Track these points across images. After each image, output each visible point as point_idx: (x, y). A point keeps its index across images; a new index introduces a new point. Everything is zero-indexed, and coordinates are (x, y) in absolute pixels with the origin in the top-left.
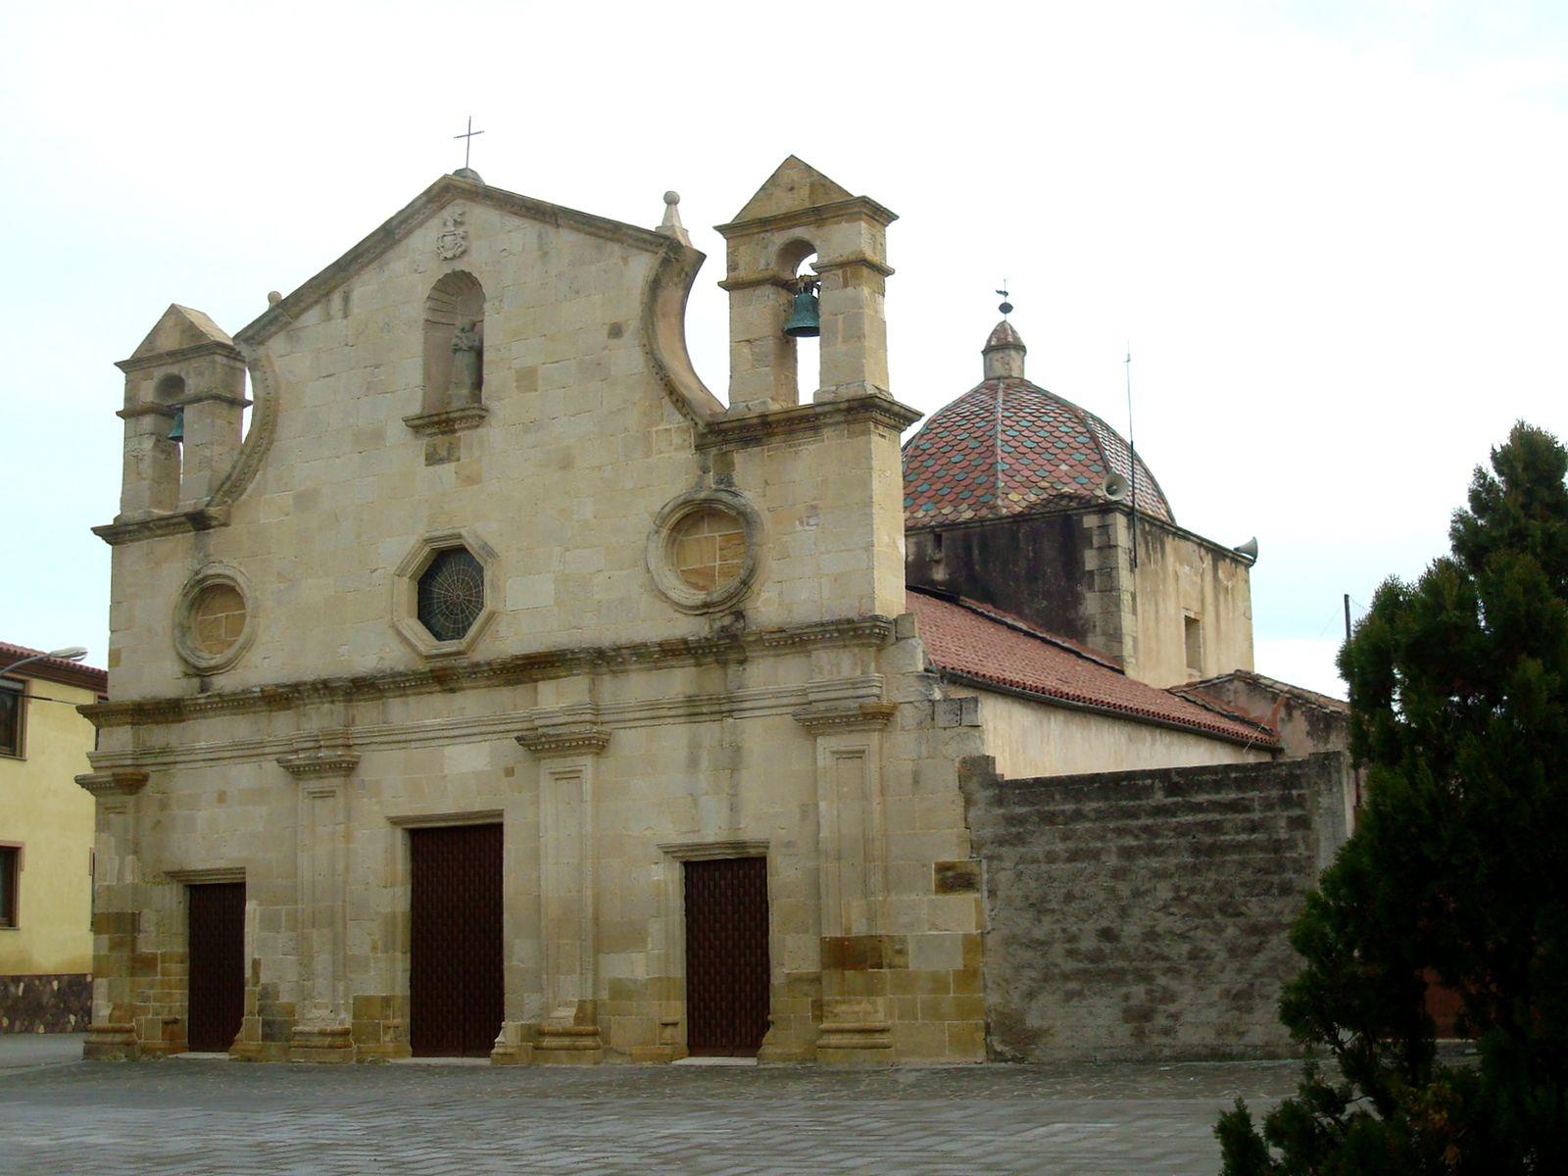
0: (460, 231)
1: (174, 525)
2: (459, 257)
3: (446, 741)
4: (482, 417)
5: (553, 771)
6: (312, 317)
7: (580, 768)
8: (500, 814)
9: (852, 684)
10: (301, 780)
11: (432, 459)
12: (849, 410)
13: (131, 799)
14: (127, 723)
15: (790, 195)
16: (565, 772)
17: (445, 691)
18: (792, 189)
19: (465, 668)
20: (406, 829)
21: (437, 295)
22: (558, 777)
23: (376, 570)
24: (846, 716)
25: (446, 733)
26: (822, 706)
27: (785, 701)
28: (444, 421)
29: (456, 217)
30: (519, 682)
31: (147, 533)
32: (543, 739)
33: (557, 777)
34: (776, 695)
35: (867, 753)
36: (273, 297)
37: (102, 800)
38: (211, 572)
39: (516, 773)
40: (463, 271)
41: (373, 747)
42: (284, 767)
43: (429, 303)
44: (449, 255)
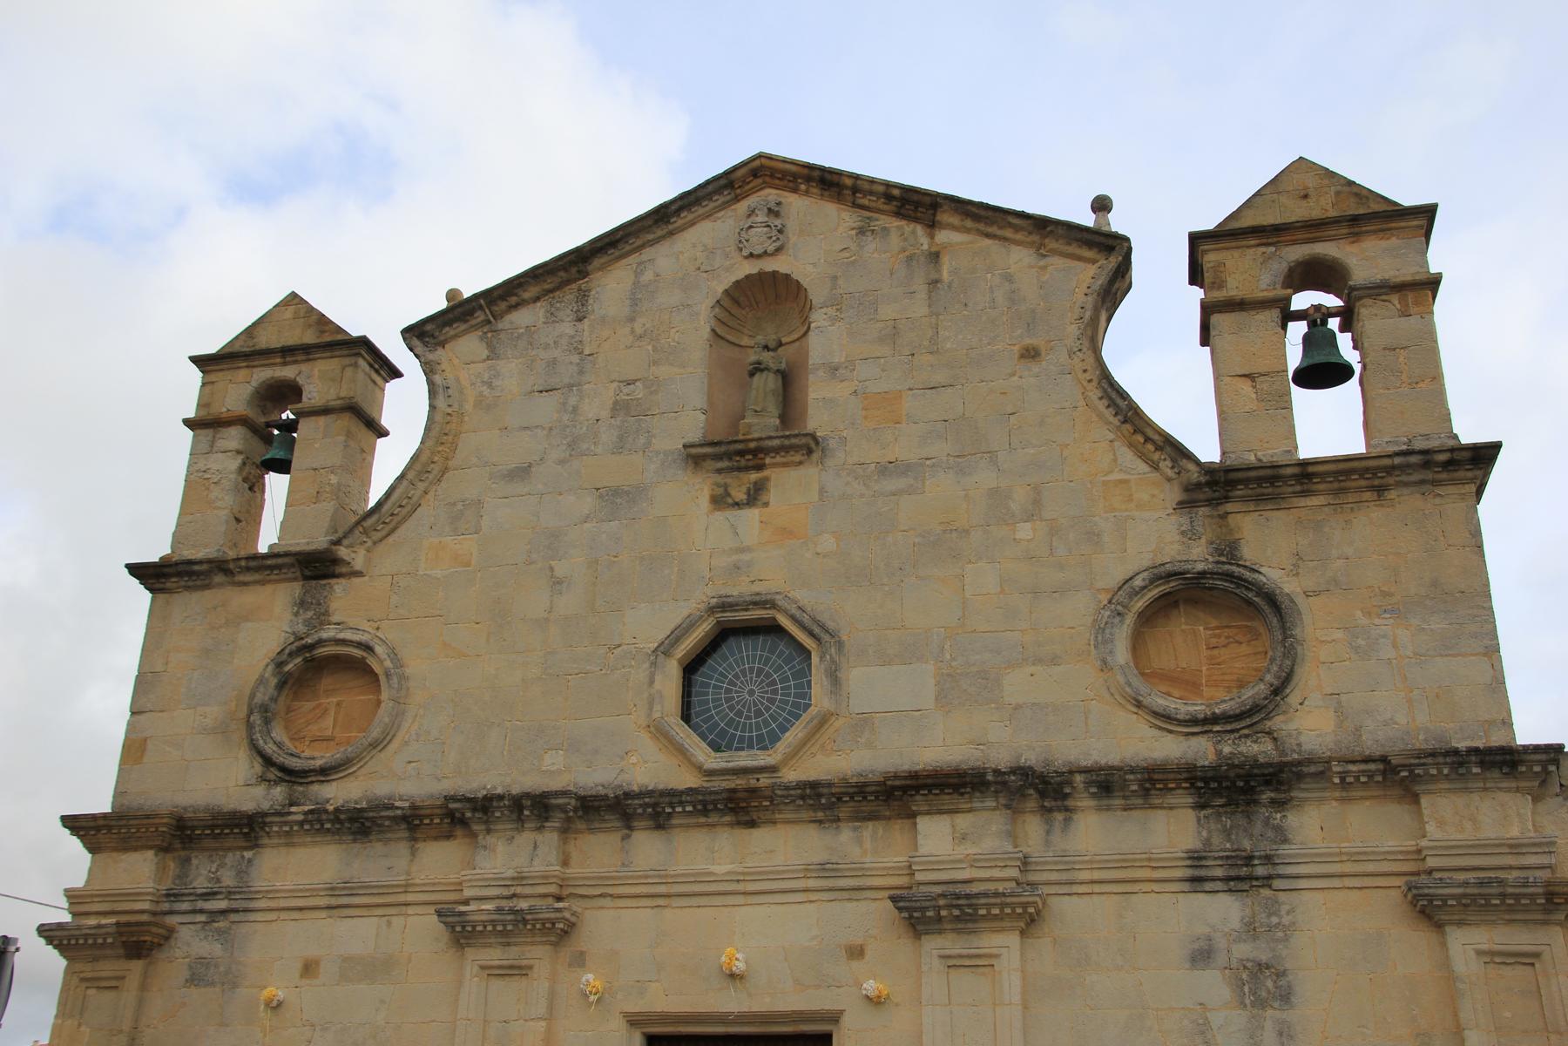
0: (778, 222)
1: (271, 568)
2: (772, 255)
3: (740, 899)
4: (810, 452)
5: (948, 952)
6: (522, 318)
7: (994, 951)
8: (835, 1018)
9: (1511, 846)
10: (469, 945)
11: (720, 501)
12: (1450, 465)
13: (137, 966)
14: (150, 848)
15: (1304, 203)
16: (961, 956)
17: (739, 823)
18: (1306, 196)
19: (787, 788)
20: (644, 1034)
21: (727, 303)
22: (953, 963)
23: (619, 646)
24: (1512, 895)
25: (740, 887)
26: (1471, 876)
27: (1371, 867)
28: (749, 451)
29: (772, 205)
30: (872, 817)
31: (219, 578)
32: (942, 902)
33: (951, 962)
34: (1355, 857)
35: (1546, 957)
36: (452, 295)
37: (79, 966)
38: (324, 635)
39: (869, 953)
40: (774, 274)
41: (607, 902)
42: (444, 923)
43: (717, 310)
44: (758, 250)
